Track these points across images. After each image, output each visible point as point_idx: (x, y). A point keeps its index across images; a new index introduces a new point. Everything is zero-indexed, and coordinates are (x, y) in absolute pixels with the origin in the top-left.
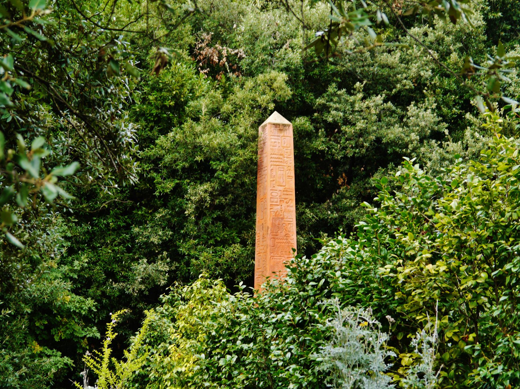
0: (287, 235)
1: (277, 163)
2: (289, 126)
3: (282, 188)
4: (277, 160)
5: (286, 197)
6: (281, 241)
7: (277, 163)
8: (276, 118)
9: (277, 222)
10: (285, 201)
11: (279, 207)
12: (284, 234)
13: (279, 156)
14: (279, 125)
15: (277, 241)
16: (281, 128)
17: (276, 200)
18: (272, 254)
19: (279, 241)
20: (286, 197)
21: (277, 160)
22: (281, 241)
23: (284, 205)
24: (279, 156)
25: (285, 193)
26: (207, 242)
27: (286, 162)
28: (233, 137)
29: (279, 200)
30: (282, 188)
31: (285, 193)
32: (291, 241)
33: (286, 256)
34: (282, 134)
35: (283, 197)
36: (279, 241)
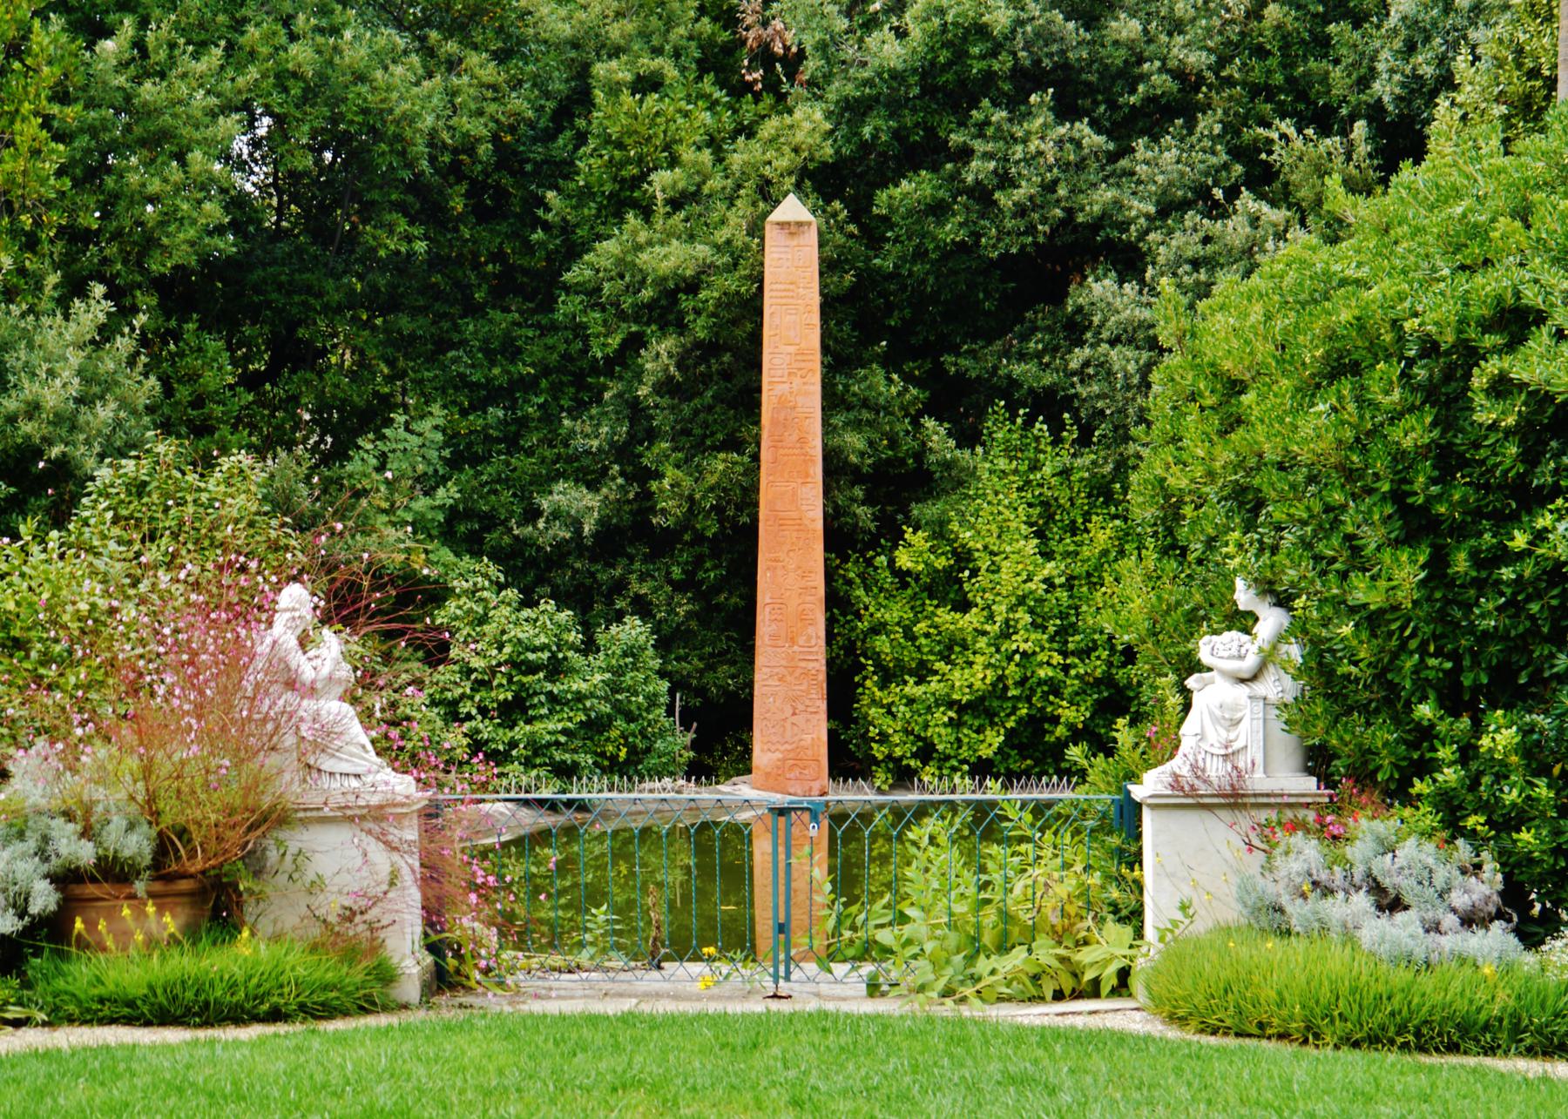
0: (802, 441)
2: (809, 224)
3: (792, 349)
5: (803, 365)
8: (792, 208)
11: (786, 386)
12: (795, 437)
14: (789, 224)
15: (781, 451)
16: (793, 229)
17: (779, 373)
20: (803, 365)
23: (797, 381)
26: (703, 443)
28: (702, 251)
30: (792, 349)
32: (812, 452)
34: (795, 242)
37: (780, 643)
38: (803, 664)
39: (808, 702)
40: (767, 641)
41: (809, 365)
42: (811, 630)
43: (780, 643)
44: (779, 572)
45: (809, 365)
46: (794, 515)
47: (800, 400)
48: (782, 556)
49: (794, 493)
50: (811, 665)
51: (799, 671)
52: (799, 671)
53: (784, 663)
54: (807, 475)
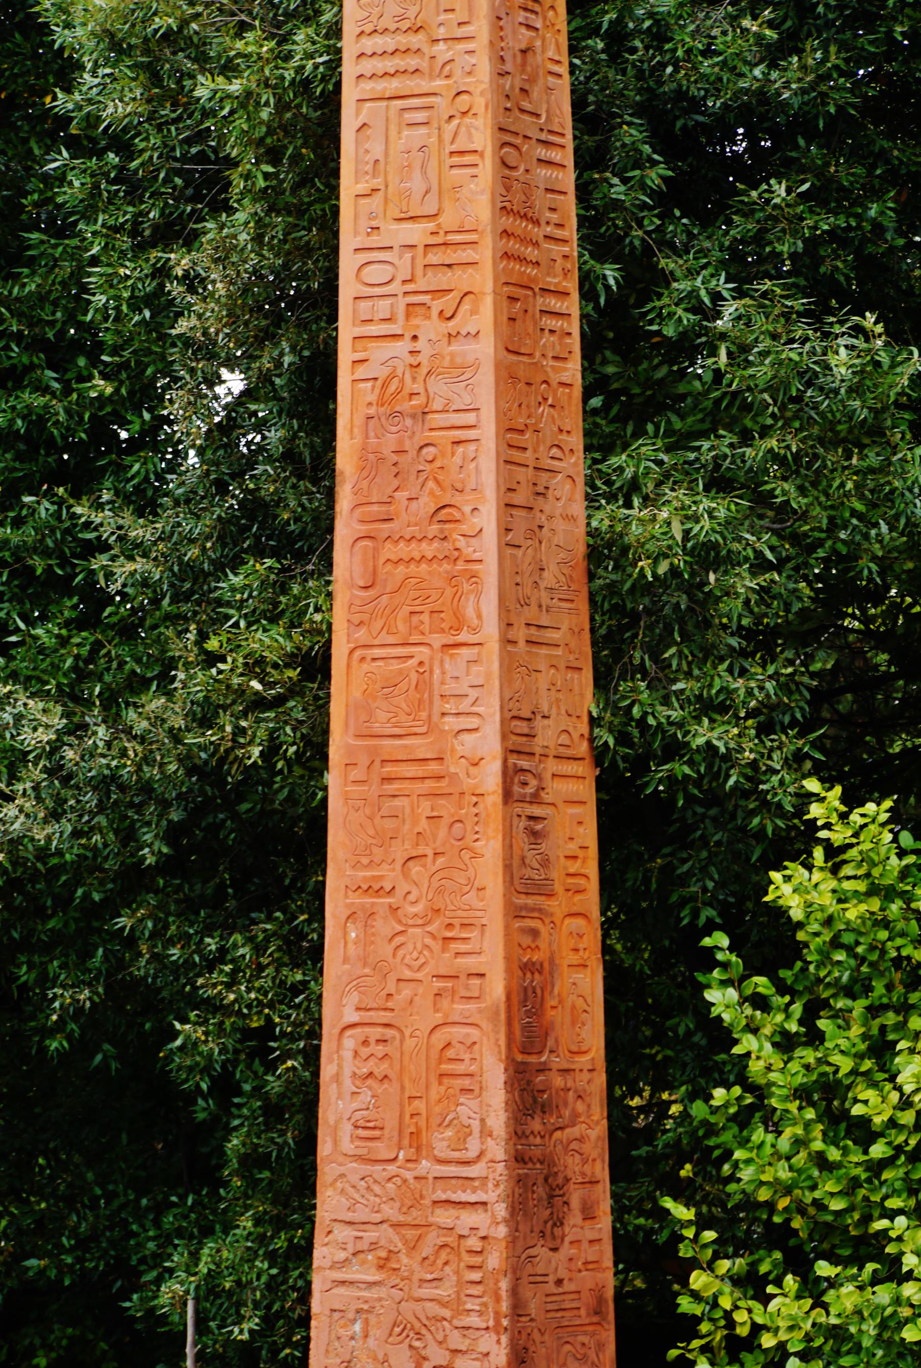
1: (393, 86)
3: (416, 233)
4: (390, 65)
5: (443, 279)
6: (415, 549)
7: (393, 86)
9: (390, 442)
10: (437, 306)
11: (401, 348)
12: (425, 505)
13: (403, 40)
15: (390, 551)
17: (383, 307)
18: (361, 635)
19: (404, 550)
20: (443, 279)
21: (390, 65)
22: (415, 549)
24: (403, 40)
25: (434, 258)
27: (445, 69)
29: (402, 302)
30: (416, 233)
31: (434, 258)
32: (469, 549)
33: (438, 640)
35: (421, 285)
36: (404, 550)
37: (383, 1150)
38: (443, 1217)
39: (456, 1340)
40: (347, 1146)
41: (460, 280)
42: (467, 1110)
43: (383, 1150)
44: (384, 927)
45: (460, 280)
46: (421, 747)
47: (439, 388)
48: (389, 875)
49: (423, 684)
50: (469, 1219)
51: (432, 1239)
52: (432, 1239)
53: (390, 1211)
54: (459, 624)
